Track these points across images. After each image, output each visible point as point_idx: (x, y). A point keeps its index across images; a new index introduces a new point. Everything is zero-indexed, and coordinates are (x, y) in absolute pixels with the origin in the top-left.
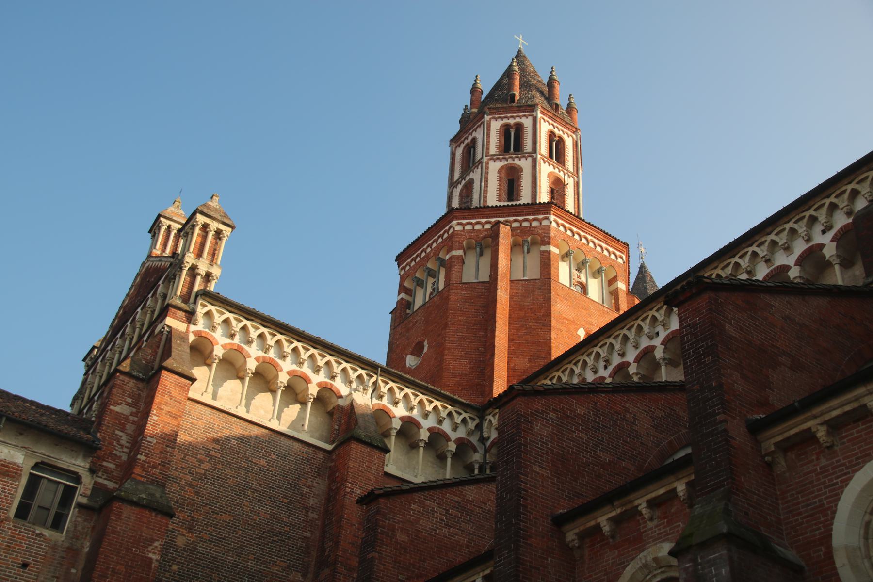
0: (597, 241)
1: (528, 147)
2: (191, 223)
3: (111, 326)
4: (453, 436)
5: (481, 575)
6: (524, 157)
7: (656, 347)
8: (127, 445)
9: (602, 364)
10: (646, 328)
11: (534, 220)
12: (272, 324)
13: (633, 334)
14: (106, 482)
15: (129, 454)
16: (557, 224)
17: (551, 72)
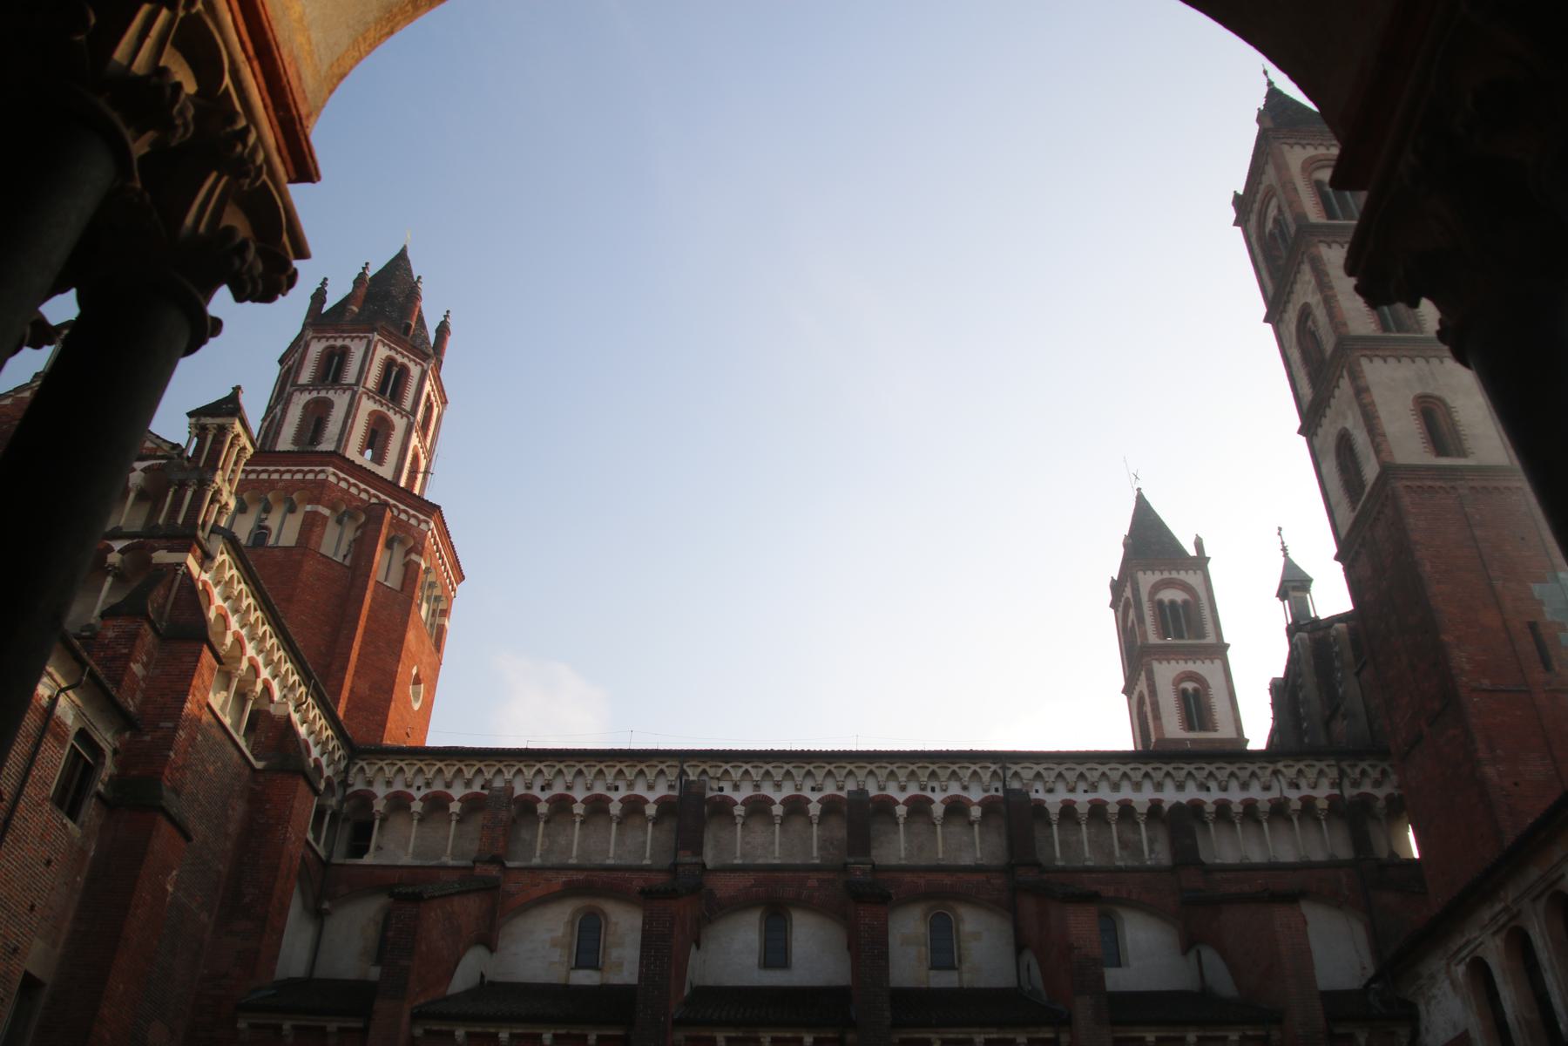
0: (448, 566)
1: (407, 404)
2: (219, 421)
5: (553, 1031)
6: (401, 413)
7: (612, 801)
9: (539, 782)
10: (610, 779)
11: (414, 516)
12: (261, 597)
13: (592, 775)
16: (433, 534)
17: (446, 317)
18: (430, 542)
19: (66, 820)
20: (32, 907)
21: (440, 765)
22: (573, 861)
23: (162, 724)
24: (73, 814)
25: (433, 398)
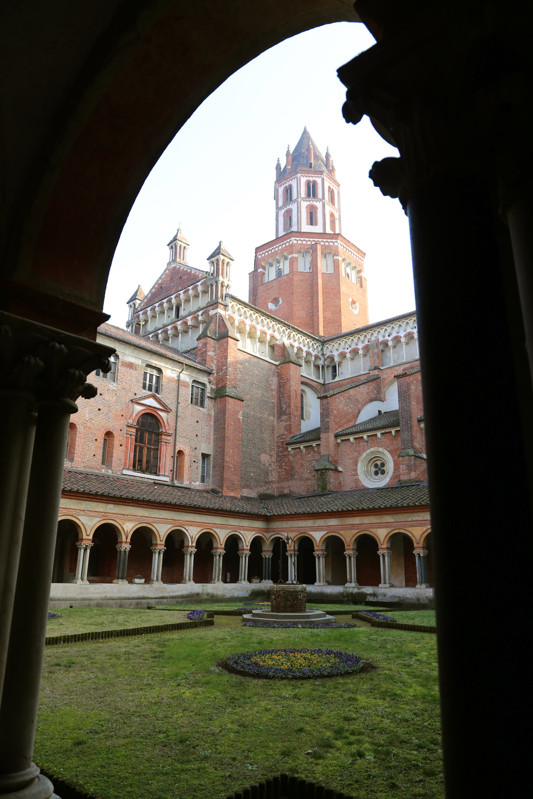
0: (355, 253)
1: (320, 196)
2: (216, 258)
3: (150, 292)
4: (313, 354)
5: (380, 432)
8: (216, 369)
9: (387, 334)
11: (331, 242)
17: (327, 150)
18: (341, 249)
19: (201, 409)
20: (197, 436)
21: (352, 338)
22: (404, 361)
23: (223, 368)
24: (202, 405)
25: (332, 187)
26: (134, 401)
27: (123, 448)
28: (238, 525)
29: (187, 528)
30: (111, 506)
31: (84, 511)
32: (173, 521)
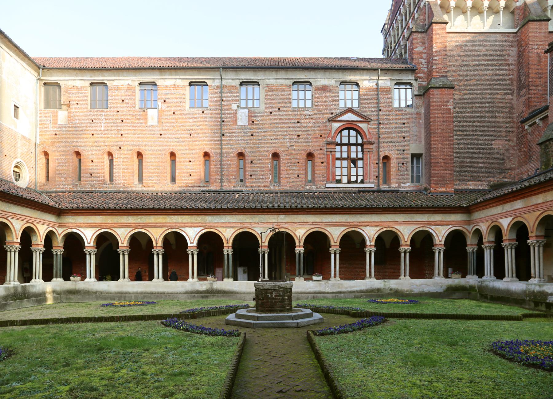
14: (422, 83)
15: (427, 67)
26: (330, 120)
27: (325, 164)
28: (427, 220)
29: (363, 228)
30: (282, 217)
31: (257, 223)
32: (347, 223)
